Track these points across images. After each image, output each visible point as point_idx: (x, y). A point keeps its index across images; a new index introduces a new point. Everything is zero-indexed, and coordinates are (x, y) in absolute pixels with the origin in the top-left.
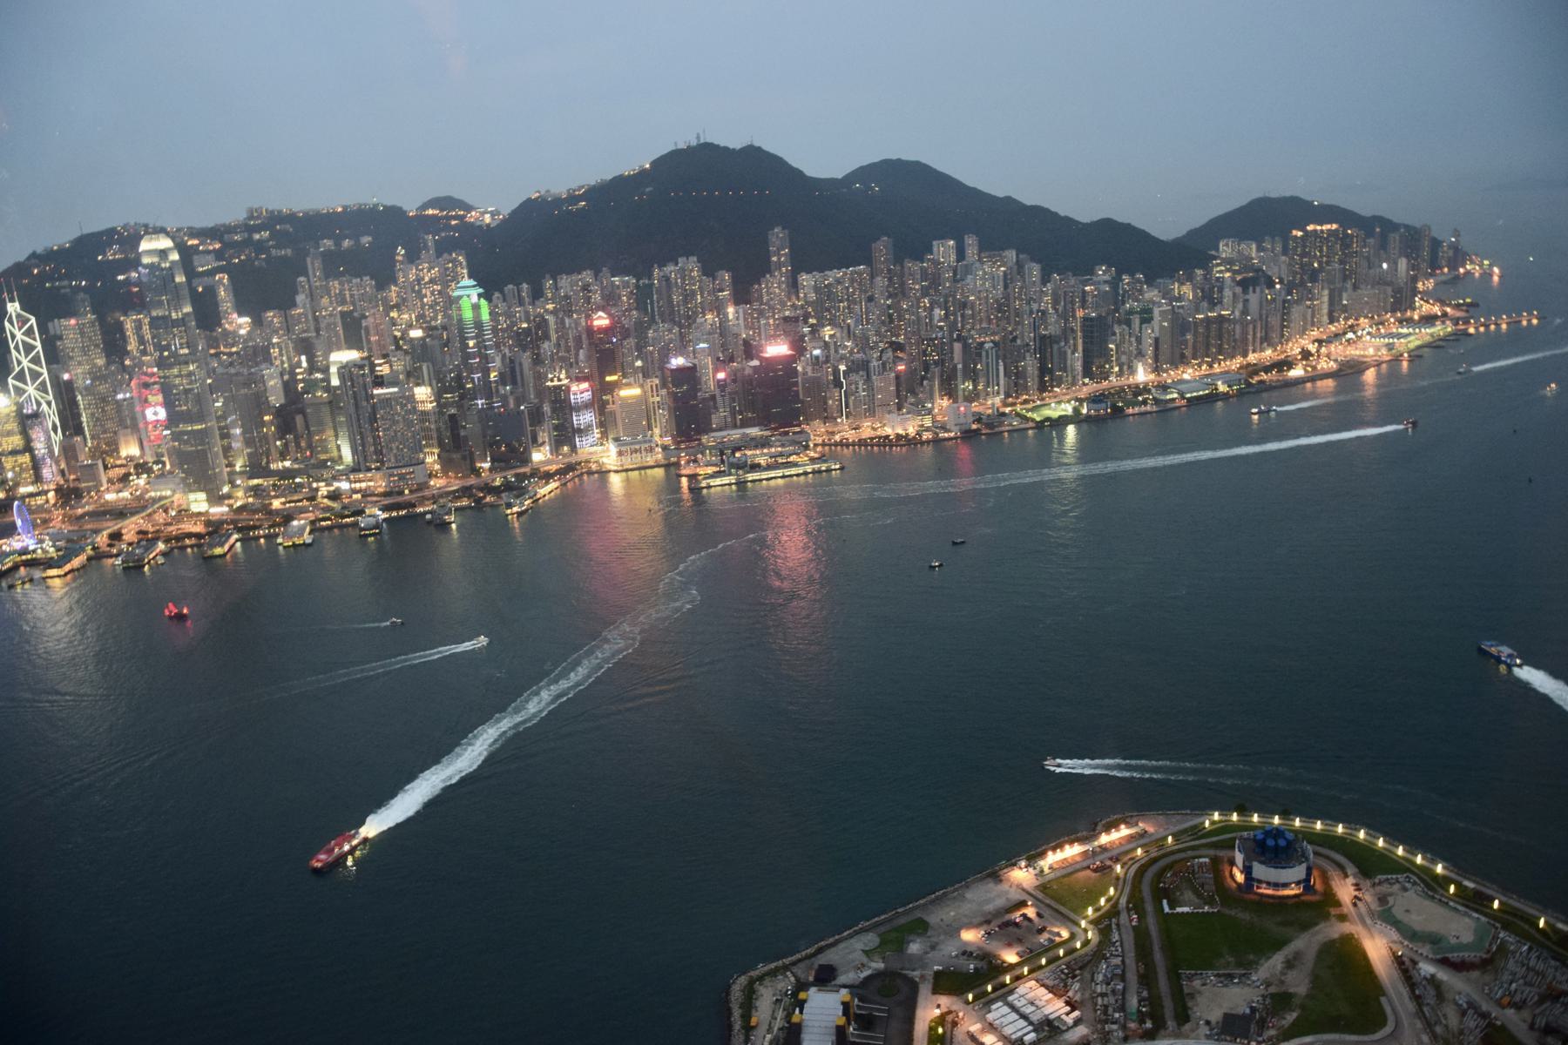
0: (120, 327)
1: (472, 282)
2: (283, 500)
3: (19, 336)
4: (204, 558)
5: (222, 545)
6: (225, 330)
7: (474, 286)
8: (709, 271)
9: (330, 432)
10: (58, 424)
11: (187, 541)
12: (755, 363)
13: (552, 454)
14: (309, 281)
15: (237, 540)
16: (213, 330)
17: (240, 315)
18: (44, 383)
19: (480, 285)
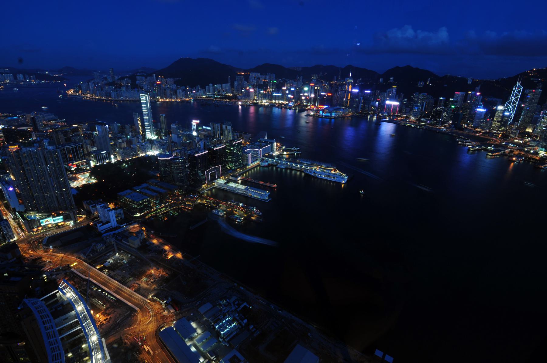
10: (513, 117)
18: (516, 105)
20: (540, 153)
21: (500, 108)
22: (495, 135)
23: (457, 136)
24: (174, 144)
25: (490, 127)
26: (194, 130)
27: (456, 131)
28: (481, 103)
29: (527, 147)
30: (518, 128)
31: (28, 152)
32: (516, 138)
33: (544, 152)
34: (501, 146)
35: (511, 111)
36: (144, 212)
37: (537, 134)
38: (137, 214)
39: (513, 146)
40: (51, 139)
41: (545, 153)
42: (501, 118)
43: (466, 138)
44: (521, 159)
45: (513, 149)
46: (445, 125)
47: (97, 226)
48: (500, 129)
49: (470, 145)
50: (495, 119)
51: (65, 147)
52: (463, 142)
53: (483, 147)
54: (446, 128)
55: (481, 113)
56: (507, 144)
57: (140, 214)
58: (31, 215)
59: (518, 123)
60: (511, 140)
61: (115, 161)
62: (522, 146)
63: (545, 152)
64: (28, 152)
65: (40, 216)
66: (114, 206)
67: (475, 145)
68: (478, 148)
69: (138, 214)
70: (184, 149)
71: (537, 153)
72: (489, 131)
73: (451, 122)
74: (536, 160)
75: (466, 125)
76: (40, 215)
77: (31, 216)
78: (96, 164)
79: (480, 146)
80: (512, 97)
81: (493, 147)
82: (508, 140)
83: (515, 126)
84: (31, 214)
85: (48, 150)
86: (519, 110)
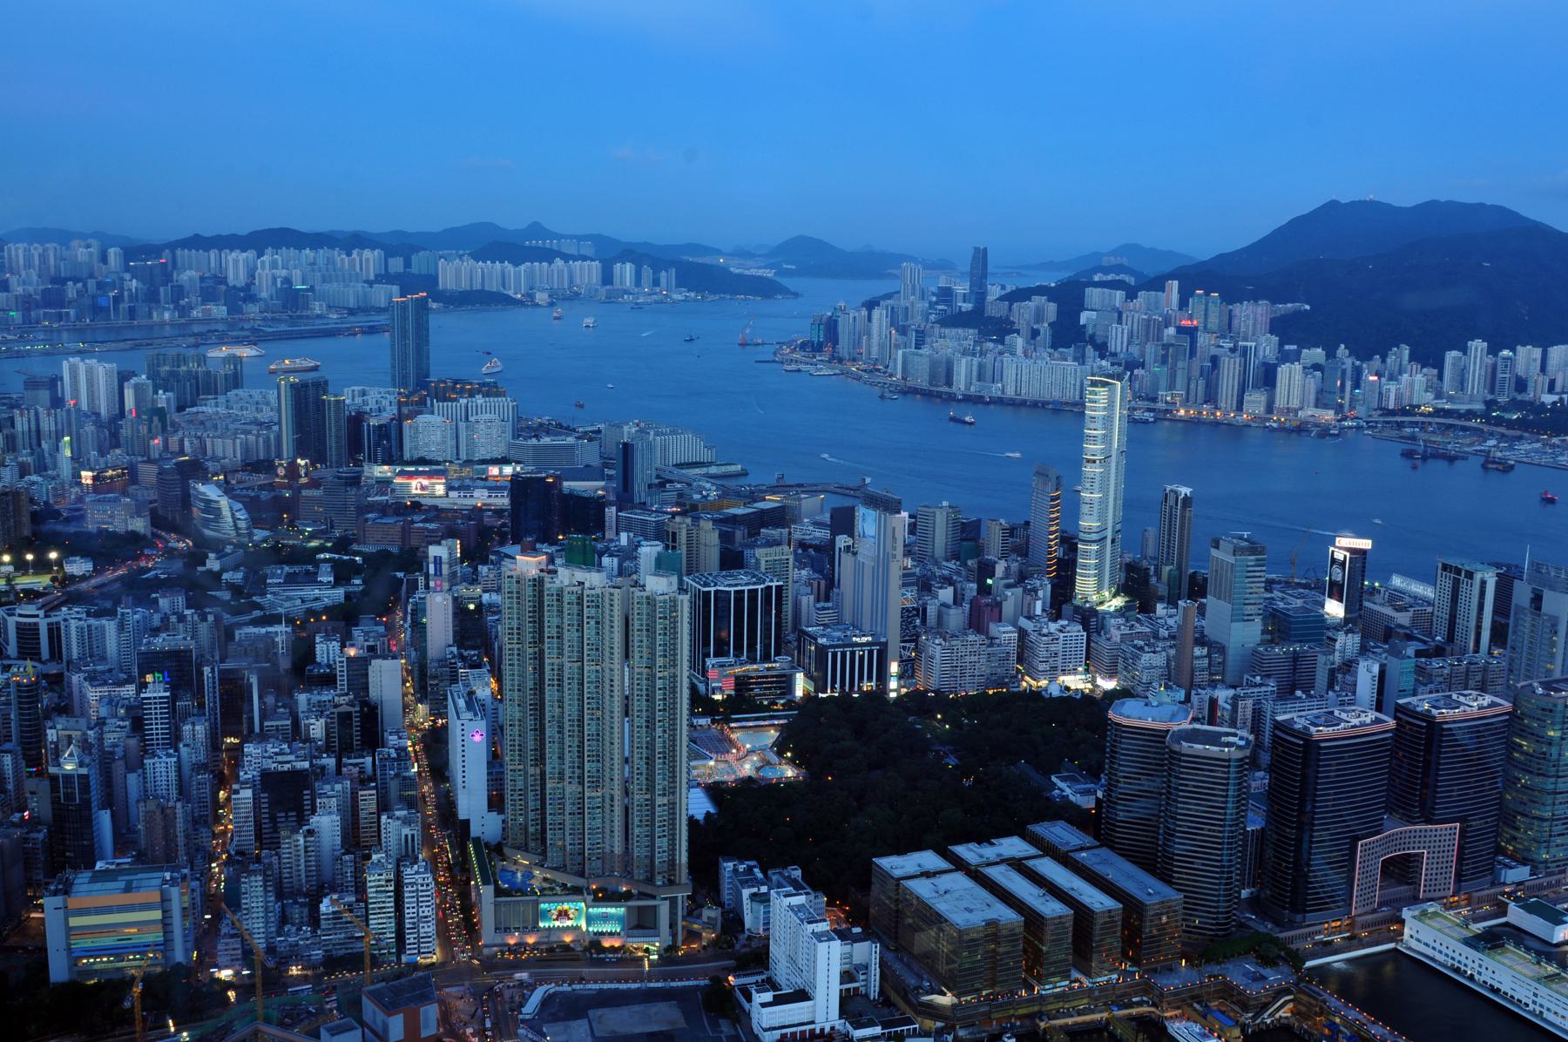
24: (1205, 651)
26: (1335, 589)
31: (575, 589)
36: (978, 990)
38: (945, 994)
40: (667, 547)
47: (749, 999)
51: (712, 589)
57: (958, 996)
58: (513, 868)
61: (904, 691)
64: (575, 589)
65: (546, 885)
66: (847, 918)
69: (949, 994)
70: (1256, 685)
76: (545, 880)
77: (514, 873)
78: (817, 691)
84: (515, 862)
85: (645, 594)
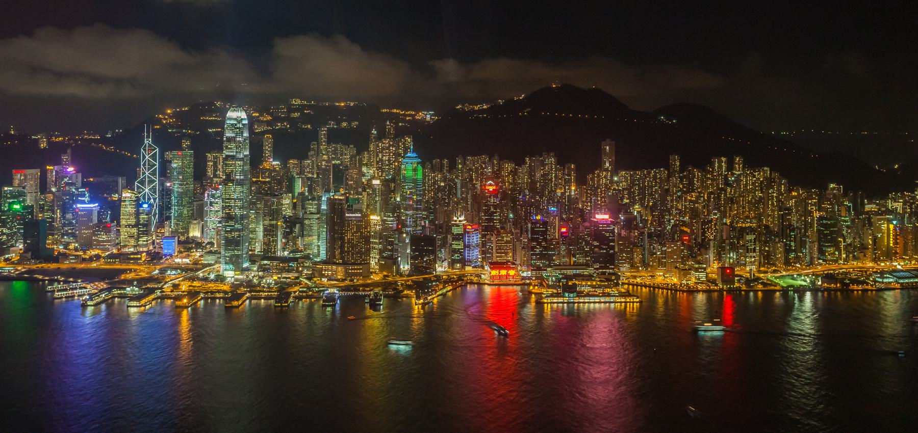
0: (205, 160)
1: (415, 155)
2: (280, 276)
3: (147, 157)
4: (226, 306)
5: (238, 300)
6: (264, 167)
7: (416, 157)
8: (562, 162)
9: (315, 237)
10: (157, 212)
11: (218, 295)
12: (587, 224)
13: (449, 268)
14: (318, 145)
15: (248, 298)
16: (257, 167)
17: (273, 161)
19: (419, 157)
20: (227, 276)
21: (127, 194)
22: (132, 256)
23: (47, 278)
25: (117, 241)
27: (40, 266)
28: (84, 190)
29: (201, 269)
30: (174, 234)
32: (176, 254)
33: (233, 273)
34: (151, 279)
35: (149, 199)
37: (211, 238)
39: (175, 274)
41: (236, 275)
42: (135, 218)
43: (71, 279)
44: (199, 298)
45: (176, 282)
46: (7, 256)
48: (139, 241)
49: (84, 290)
50: (123, 222)
52: (66, 290)
53: (116, 292)
54: (13, 263)
55: (90, 212)
56: (163, 271)
59: (171, 223)
60: (167, 262)
62: (191, 270)
63: (235, 271)
67: (96, 291)
68: (103, 295)
71: (220, 279)
72: (119, 250)
73: (21, 246)
74: (225, 292)
75: (61, 247)
79: (109, 290)
80: (143, 170)
81: (136, 286)
82: (162, 263)
83: (167, 231)
86: (165, 193)
